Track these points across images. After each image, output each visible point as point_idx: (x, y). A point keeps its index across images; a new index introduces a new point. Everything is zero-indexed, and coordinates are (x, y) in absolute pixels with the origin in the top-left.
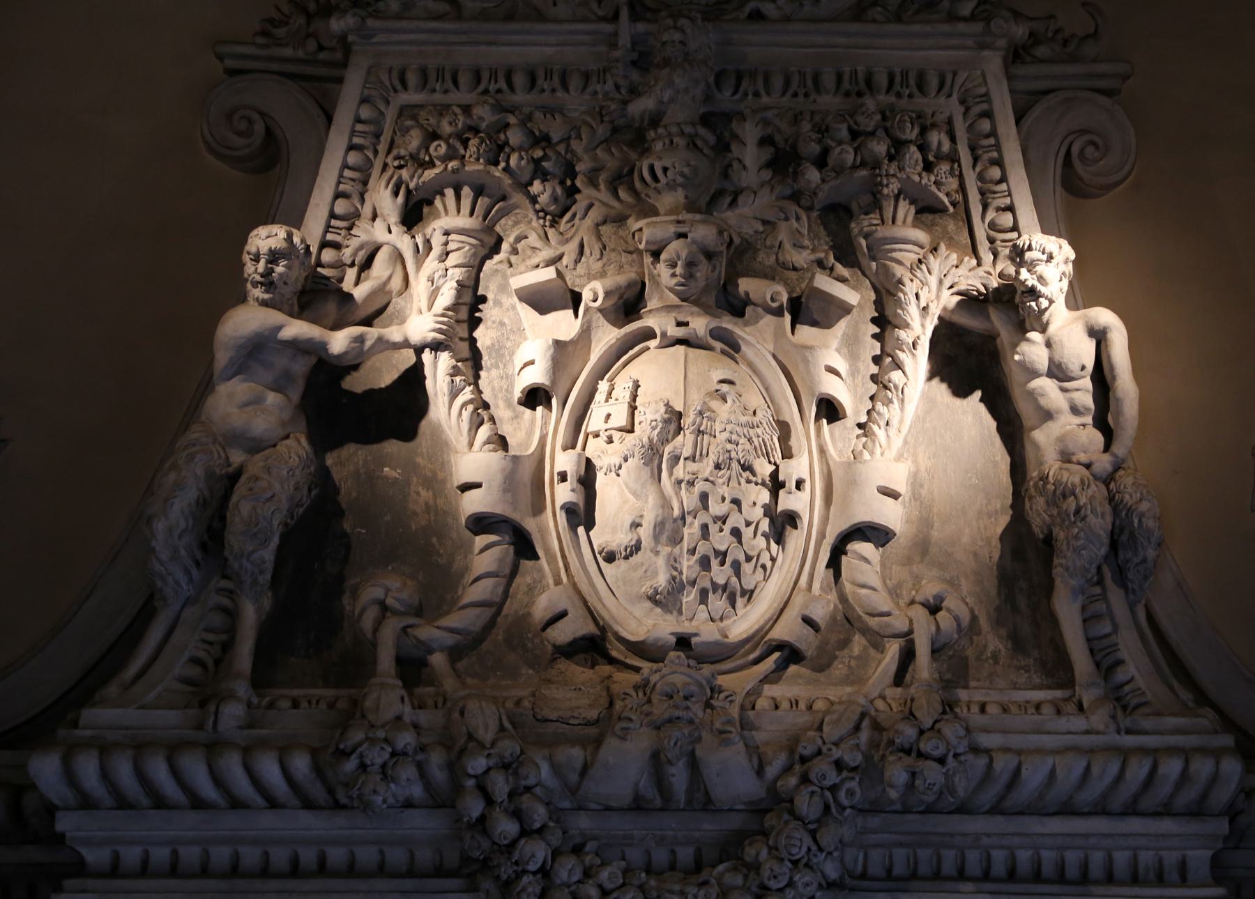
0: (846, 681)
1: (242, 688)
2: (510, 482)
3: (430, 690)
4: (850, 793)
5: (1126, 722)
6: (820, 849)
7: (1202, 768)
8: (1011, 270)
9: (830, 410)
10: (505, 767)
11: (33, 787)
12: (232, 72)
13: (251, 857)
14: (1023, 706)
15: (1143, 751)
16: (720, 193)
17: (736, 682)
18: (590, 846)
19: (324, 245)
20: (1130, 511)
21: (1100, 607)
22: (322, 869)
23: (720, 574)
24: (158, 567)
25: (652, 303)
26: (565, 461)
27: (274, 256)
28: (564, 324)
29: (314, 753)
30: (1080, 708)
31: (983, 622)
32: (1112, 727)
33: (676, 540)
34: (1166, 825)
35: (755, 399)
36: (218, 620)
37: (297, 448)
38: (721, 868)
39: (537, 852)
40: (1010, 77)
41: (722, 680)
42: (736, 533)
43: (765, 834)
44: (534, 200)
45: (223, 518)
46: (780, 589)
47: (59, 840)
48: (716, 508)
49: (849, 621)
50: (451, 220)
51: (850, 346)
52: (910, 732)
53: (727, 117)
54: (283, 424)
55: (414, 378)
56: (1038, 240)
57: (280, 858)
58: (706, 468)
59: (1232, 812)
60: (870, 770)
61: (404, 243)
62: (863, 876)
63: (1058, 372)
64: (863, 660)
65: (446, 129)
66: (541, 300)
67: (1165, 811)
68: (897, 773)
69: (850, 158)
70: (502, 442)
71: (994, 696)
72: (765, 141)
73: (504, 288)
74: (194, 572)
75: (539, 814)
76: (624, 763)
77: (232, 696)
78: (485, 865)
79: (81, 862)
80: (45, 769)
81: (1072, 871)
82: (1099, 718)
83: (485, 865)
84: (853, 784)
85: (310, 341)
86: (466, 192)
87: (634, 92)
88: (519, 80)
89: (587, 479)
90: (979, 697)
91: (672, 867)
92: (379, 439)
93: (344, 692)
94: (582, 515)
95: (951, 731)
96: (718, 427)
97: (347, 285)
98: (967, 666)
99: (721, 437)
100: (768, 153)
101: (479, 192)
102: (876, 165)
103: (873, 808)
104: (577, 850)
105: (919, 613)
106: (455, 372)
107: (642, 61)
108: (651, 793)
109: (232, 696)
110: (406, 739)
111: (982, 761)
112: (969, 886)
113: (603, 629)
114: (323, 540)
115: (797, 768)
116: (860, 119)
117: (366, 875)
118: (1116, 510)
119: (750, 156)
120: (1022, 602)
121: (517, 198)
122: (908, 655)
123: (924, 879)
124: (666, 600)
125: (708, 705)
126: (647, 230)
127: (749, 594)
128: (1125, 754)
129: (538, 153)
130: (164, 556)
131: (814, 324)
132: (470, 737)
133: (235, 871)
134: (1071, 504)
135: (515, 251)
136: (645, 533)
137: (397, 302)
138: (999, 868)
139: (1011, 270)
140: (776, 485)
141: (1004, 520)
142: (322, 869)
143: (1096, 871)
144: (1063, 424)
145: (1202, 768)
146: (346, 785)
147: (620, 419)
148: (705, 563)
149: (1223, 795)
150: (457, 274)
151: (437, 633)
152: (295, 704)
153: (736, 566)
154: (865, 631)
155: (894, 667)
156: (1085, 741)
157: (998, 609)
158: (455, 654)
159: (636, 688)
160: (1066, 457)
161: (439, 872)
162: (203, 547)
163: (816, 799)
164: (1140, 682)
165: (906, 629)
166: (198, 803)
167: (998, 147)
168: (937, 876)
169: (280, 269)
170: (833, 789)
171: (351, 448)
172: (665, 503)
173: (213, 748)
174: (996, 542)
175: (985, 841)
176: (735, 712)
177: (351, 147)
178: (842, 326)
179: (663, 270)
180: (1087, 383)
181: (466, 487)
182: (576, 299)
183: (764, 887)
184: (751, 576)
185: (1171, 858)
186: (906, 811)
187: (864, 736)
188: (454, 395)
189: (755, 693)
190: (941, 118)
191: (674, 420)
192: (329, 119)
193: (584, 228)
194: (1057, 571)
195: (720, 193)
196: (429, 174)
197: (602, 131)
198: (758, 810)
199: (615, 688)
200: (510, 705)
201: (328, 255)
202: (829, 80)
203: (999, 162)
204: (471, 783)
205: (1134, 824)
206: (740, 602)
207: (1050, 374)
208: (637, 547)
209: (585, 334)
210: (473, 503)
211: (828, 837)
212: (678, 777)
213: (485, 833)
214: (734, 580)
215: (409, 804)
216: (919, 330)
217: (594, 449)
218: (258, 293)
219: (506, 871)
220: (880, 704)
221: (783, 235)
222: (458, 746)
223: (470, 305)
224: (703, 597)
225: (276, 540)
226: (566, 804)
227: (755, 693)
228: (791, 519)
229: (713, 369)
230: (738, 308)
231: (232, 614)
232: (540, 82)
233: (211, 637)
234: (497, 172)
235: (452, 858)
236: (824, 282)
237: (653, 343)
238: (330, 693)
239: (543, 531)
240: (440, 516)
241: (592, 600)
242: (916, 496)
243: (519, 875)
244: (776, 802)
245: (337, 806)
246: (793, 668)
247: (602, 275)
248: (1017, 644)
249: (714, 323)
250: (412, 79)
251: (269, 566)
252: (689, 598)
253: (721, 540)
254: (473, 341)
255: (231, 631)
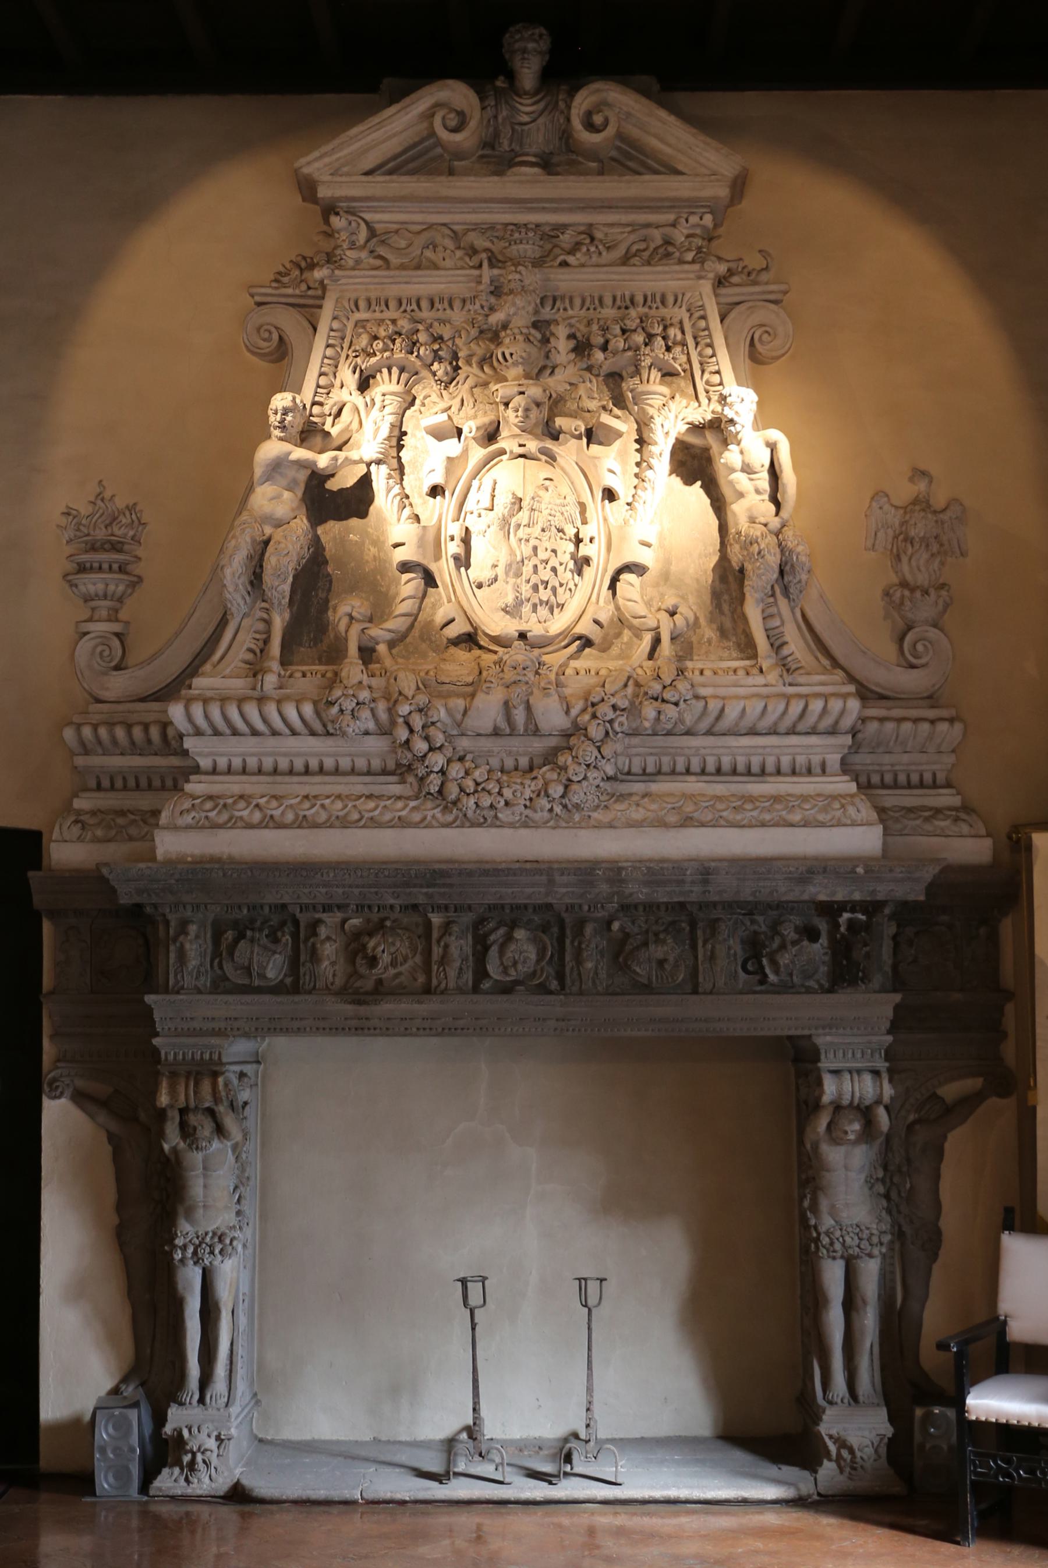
0: (620, 657)
1: (275, 666)
2: (421, 543)
3: (378, 665)
4: (621, 724)
5: (788, 679)
6: (603, 758)
7: (836, 705)
8: (719, 409)
9: (610, 495)
10: (420, 710)
11: (171, 723)
12: (259, 304)
13: (283, 764)
14: (726, 671)
15: (799, 696)
16: (543, 368)
17: (554, 659)
18: (469, 757)
19: (314, 404)
20: (791, 551)
21: (773, 610)
22: (321, 771)
23: (544, 594)
24: (228, 596)
25: (504, 432)
26: (455, 529)
27: (286, 411)
28: (452, 447)
29: (315, 703)
30: (761, 671)
31: (702, 621)
32: (781, 682)
33: (518, 574)
34: (813, 740)
35: (565, 489)
36: (261, 626)
37: (301, 524)
38: (544, 769)
39: (438, 760)
40: (716, 295)
41: (545, 658)
42: (554, 570)
43: (570, 749)
44: (434, 374)
45: (261, 566)
46: (581, 604)
47: (185, 753)
48: (542, 555)
49: (621, 621)
50: (386, 386)
51: (622, 455)
52: (657, 687)
53: (548, 323)
54: (293, 510)
55: (366, 481)
56: (732, 388)
57: (299, 764)
58: (536, 531)
59: (854, 733)
60: (633, 710)
61: (357, 399)
62: (629, 773)
63: (747, 469)
64: (629, 645)
65: (382, 333)
66: (439, 434)
67: (813, 732)
68: (649, 711)
69: (621, 345)
70: (417, 518)
71: (707, 665)
72: (571, 336)
73: (417, 426)
74: (247, 598)
75: (439, 739)
76: (488, 708)
77: (270, 670)
78: (409, 768)
79: (198, 766)
80: (176, 712)
81: (755, 769)
82: (772, 677)
83: (409, 768)
84: (623, 719)
85: (307, 460)
86: (395, 371)
87: (492, 309)
88: (424, 304)
89: (466, 541)
90: (699, 665)
91: (516, 769)
92: (346, 518)
93: (331, 668)
94: (463, 561)
95: (682, 686)
96: (543, 506)
97: (327, 427)
98: (692, 648)
99: (545, 512)
100: (572, 344)
101: (402, 370)
102: (637, 349)
103: (634, 733)
104: (461, 759)
105: (664, 617)
106: (390, 477)
107: (497, 291)
108: (503, 725)
109: (270, 670)
110: (364, 695)
111: (702, 703)
112: (693, 778)
113: (476, 629)
114: (314, 578)
115: (590, 709)
116: (627, 322)
117: (345, 774)
118: (782, 552)
119: (562, 345)
120: (726, 607)
121: (425, 373)
122: (657, 641)
123: (666, 774)
124: (511, 611)
125: (537, 673)
126: (501, 390)
127: (561, 606)
128: (788, 698)
129: (436, 347)
130: (231, 589)
131: (600, 443)
132: (400, 693)
133: (275, 771)
134: (755, 548)
135: (423, 405)
136: (500, 571)
137: (355, 437)
138: (711, 767)
139: (719, 409)
140: (578, 541)
141: (715, 558)
142: (321, 771)
143: (770, 767)
144: (750, 503)
145: (836, 705)
146: (333, 722)
147: (488, 505)
148: (535, 588)
149: (847, 722)
150: (391, 419)
151: (380, 632)
152: (304, 675)
153: (554, 590)
154: (631, 627)
155: (648, 649)
156: (764, 691)
157: (711, 613)
158: (392, 644)
159: (495, 663)
160: (752, 520)
161: (384, 772)
162: (251, 583)
163: (601, 728)
164: (798, 655)
165: (655, 625)
166: (255, 733)
167: (710, 336)
168: (673, 772)
169: (289, 418)
170: (611, 722)
171: (331, 523)
172: (512, 553)
173: (261, 700)
174: (710, 573)
175: (703, 751)
176: (552, 677)
177: (328, 346)
178: (617, 444)
179: (510, 413)
180: (765, 475)
181: (396, 545)
182: (459, 432)
183: (569, 780)
184: (562, 595)
185: (816, 760)
186: (655, 734)
187: (630, 690)
188: (389, 491)
189: (565, 665)
190: (675, 320)
191: (518, 502)
192: (315, 329)
193: (462, 389)
194: (747, 589)
195: (543, 368)
196: (373, 360)
197: (474, 332)
198: (567, 735)
199: (483, 664)
200: (422, 674)
201: (316, 410)
202: (608, 301)
203: (710, 345)
204: (401, 720)
205: (794, 740)
206: (556, 611)
207: (743, 470)
208: (496, 579)
209: (465, 452)
210: (400, 555)
211: (607, 751)
212: (519, 716)
213: (409, 749)
214: (553, 598)
215: (367, 733)
216: (662, 447)
217: (471, 522)
218: (277, 433)
219: (421, 772)
220: (640, 671)
221: (582, 391)
222: (393, 699)
223: (398, 437)
224: (535, 606)
225: (291, 579)
226: (455, 732)
227: (565, 665)
228: (587, 561)
229: (539, 471)
230: (555, 436)
231: (268, 622)
232: (437, 305)
233: (258, 636)
234: (412, 358)
235: (391, 765)
236: (606, 419)
237: (505, 457)
238: (323, 668)
239: (440, 571)
240: (381, 563)
241: (469, 612)
242: (661, 546)
243: (428, 774)
244: (577, 730)
245: (328, 734)
246: (587, 650)
247: (475, 417)
248: (723, 633)
249: (541, 445)
250: (362, 304)
251: (287, 594)
252: (526, 609)
253: (545, 574)
254: (399, 458)
255: (268, 632)
